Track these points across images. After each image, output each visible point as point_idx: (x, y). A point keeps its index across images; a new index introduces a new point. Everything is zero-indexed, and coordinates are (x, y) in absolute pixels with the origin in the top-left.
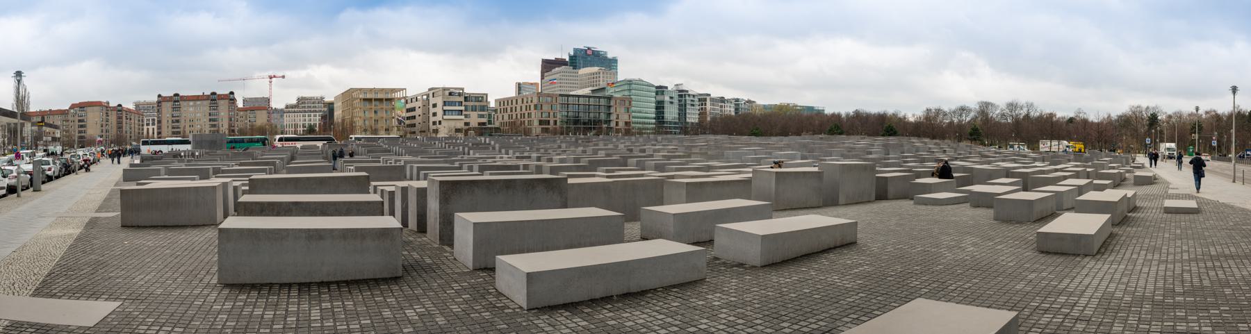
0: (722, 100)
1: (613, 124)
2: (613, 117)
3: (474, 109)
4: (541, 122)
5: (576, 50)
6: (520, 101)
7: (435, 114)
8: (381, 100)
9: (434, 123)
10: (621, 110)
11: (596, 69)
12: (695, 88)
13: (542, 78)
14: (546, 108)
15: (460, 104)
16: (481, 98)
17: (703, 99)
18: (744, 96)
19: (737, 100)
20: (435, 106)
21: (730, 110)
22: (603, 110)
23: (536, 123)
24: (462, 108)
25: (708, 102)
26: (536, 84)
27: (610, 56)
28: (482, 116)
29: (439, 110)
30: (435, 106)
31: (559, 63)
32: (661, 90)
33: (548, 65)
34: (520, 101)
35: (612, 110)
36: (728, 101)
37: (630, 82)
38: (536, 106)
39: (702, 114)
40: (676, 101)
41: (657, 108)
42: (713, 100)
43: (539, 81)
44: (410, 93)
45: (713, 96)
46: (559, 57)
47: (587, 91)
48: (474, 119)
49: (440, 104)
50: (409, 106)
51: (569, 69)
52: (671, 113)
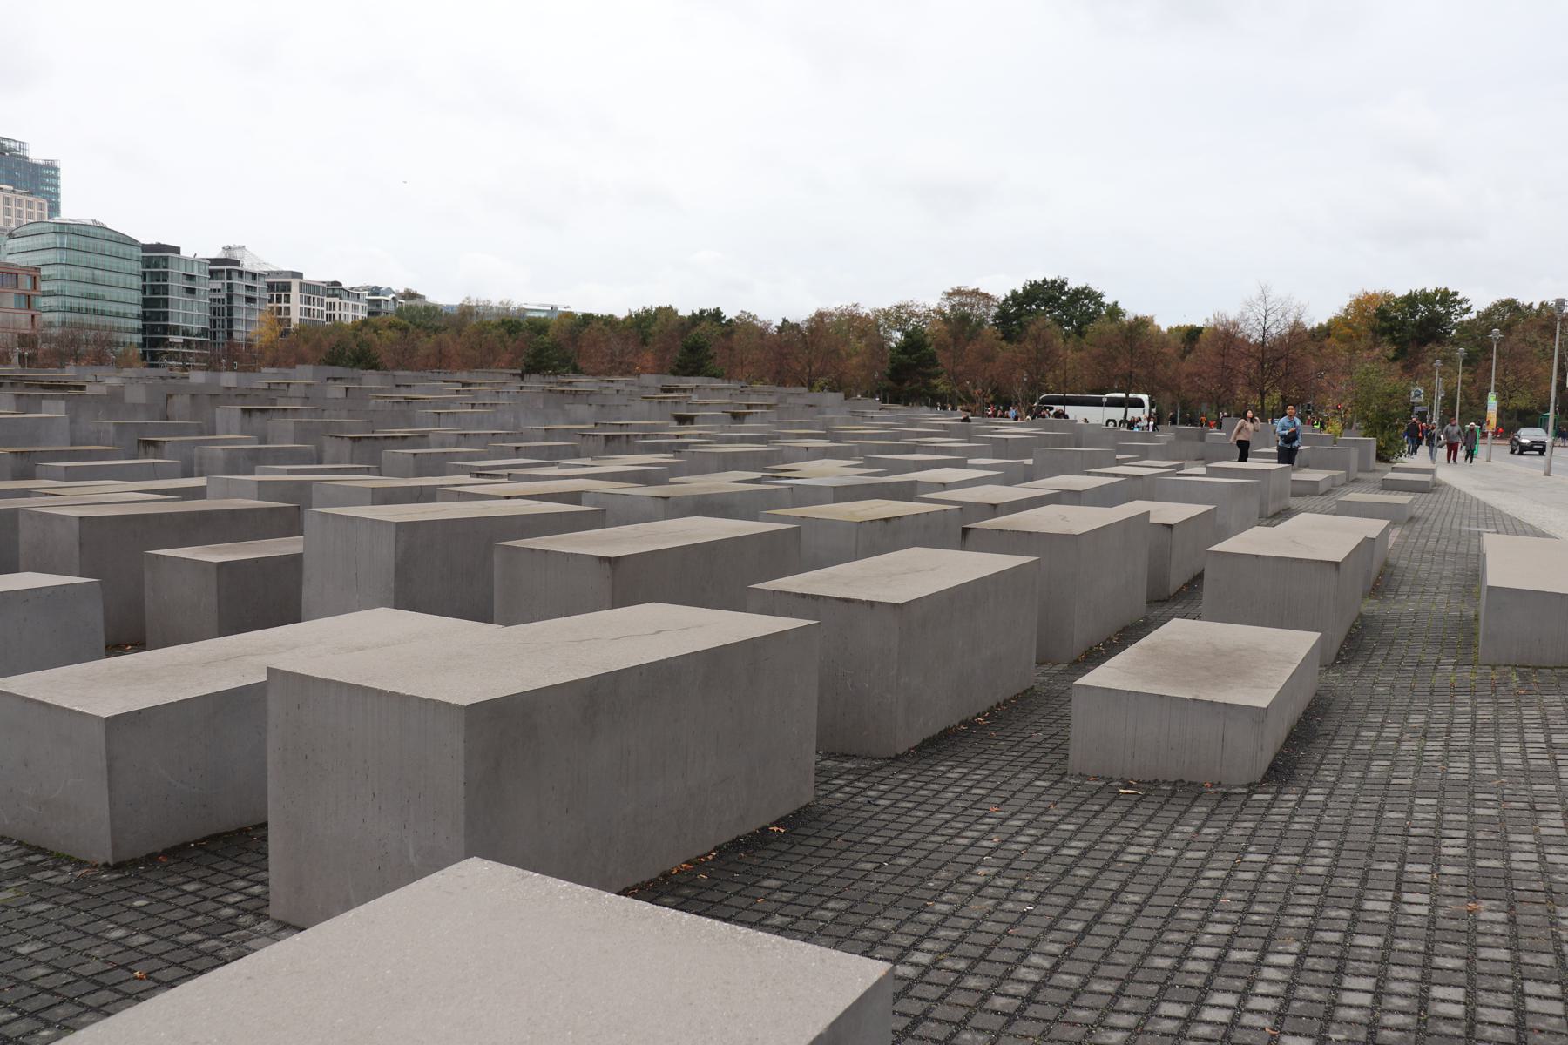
0: (335, 289)
12: (266, 253)
17: (279, 286)
18: (395, 278)
19: (375, 291)
21: (353, 313)
25: (295, 293)
32: (157, 259)
36: (348, 293)
41: (146, 303)
45: (307, 277)
52: (189, 314)
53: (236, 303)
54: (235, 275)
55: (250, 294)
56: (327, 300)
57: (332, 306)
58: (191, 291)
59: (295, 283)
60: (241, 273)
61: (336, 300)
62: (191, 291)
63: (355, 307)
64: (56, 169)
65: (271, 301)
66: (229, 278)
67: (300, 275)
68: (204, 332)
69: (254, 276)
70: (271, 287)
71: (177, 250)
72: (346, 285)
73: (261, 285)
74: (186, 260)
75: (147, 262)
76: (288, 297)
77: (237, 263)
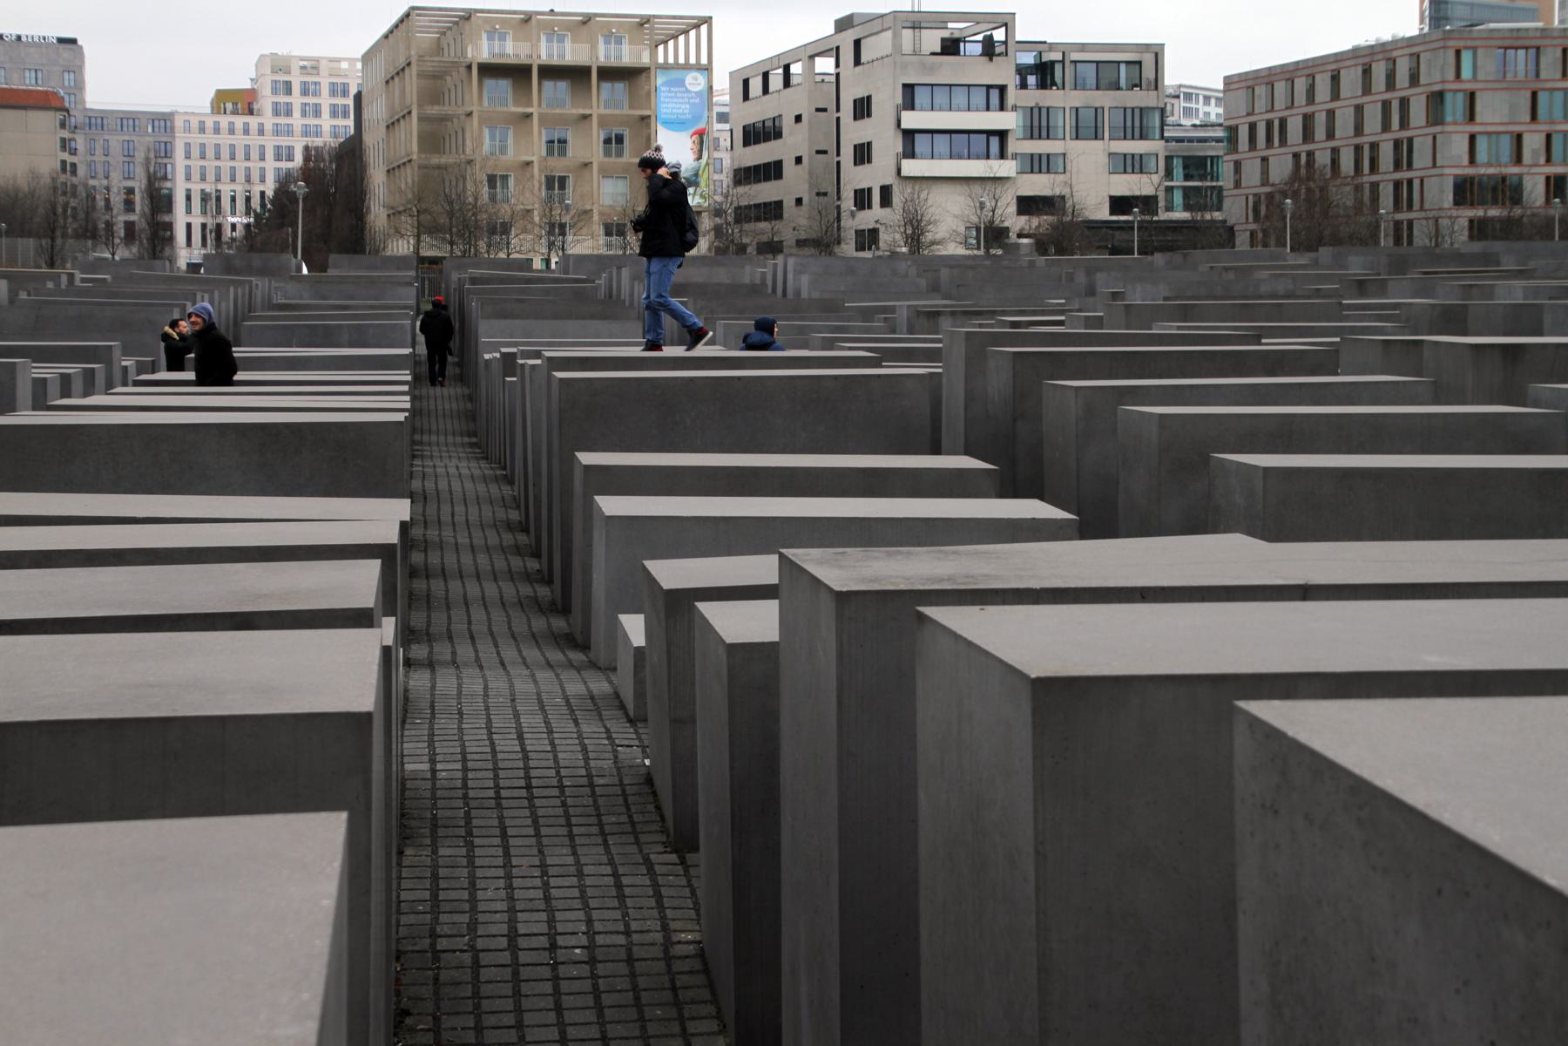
3: (1088, 127)
6: (1351, 80)
7: (863, 154)
8: (576, 75)
9: (862, 199)
15: (997, 96)
16: (1135, 68)
20: (863, 108)
24: (1006, 120)
28: (1133, 164)
29: (880, 132)
30: (863, 108)
34: (1351, 80)
38: (1437, 99)
44: (740, 45)
48: (1091, 180)
49: (886, 100)
50: (759, 111)
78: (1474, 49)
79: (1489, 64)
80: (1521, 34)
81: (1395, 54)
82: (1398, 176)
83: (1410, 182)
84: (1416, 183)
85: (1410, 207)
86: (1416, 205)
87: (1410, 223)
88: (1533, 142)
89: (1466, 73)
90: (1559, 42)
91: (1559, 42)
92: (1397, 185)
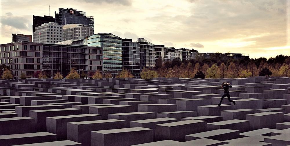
0: (173, 50)
1: (88, 69)
2: (87, 63)
4: (26, 67)
5: (60, 9)
10: (94, 57)
11: (76, 26)
13: (34, 31)
14: (30, 54)
17: (159, 48)
19: (184, 50)
22: (79, 58)
23: (22, 67)
25: (162, 52)
26: (30, 36)
27: (88, 15)
31: (47, 19)
33: (38, 21)
35: (87, 57)
37: (103, 36)
39: (159, 60)
40: (138, 51)
42: (166, 49)
43: (31, 33)
46: (48, 15)
47: (68, 42)
51: (56, 24)
53: (147, 55)
54: (146, 47)
55: (151, 52)
56: (172, 53)
57: (172, 55)
58: (135, 52)
59: (162, 48)
60: (148, 46)
61: (174, 53)
62: (135, 52)
63: (179, 55)
64: (93, 19)
65: (156, 54)
66: (145, 48)
67: (163, 46)
68: (138, 64)
69: (152, 47)
70: (157, 50)
71: (131, 40)
72: (176, 48)
73: (153, 49)
74: (134, 43)
75: (123, 44)
76: (160, 53)
77: (147, 43)
78: (26, 45)
79: (28, 48)
80: (33, 43)
81: (15, 45)
82: (15, 64)
83: (17, 65)
84: (18, 65)
85: (17, 69)
86: (18, 68)
87: (18, 71)
88: (35, 60)
89: (25, 49)
90: (39, 45)
91: (39, 45)
92: (15, 65)
